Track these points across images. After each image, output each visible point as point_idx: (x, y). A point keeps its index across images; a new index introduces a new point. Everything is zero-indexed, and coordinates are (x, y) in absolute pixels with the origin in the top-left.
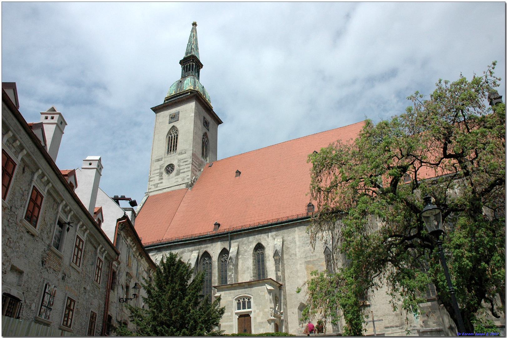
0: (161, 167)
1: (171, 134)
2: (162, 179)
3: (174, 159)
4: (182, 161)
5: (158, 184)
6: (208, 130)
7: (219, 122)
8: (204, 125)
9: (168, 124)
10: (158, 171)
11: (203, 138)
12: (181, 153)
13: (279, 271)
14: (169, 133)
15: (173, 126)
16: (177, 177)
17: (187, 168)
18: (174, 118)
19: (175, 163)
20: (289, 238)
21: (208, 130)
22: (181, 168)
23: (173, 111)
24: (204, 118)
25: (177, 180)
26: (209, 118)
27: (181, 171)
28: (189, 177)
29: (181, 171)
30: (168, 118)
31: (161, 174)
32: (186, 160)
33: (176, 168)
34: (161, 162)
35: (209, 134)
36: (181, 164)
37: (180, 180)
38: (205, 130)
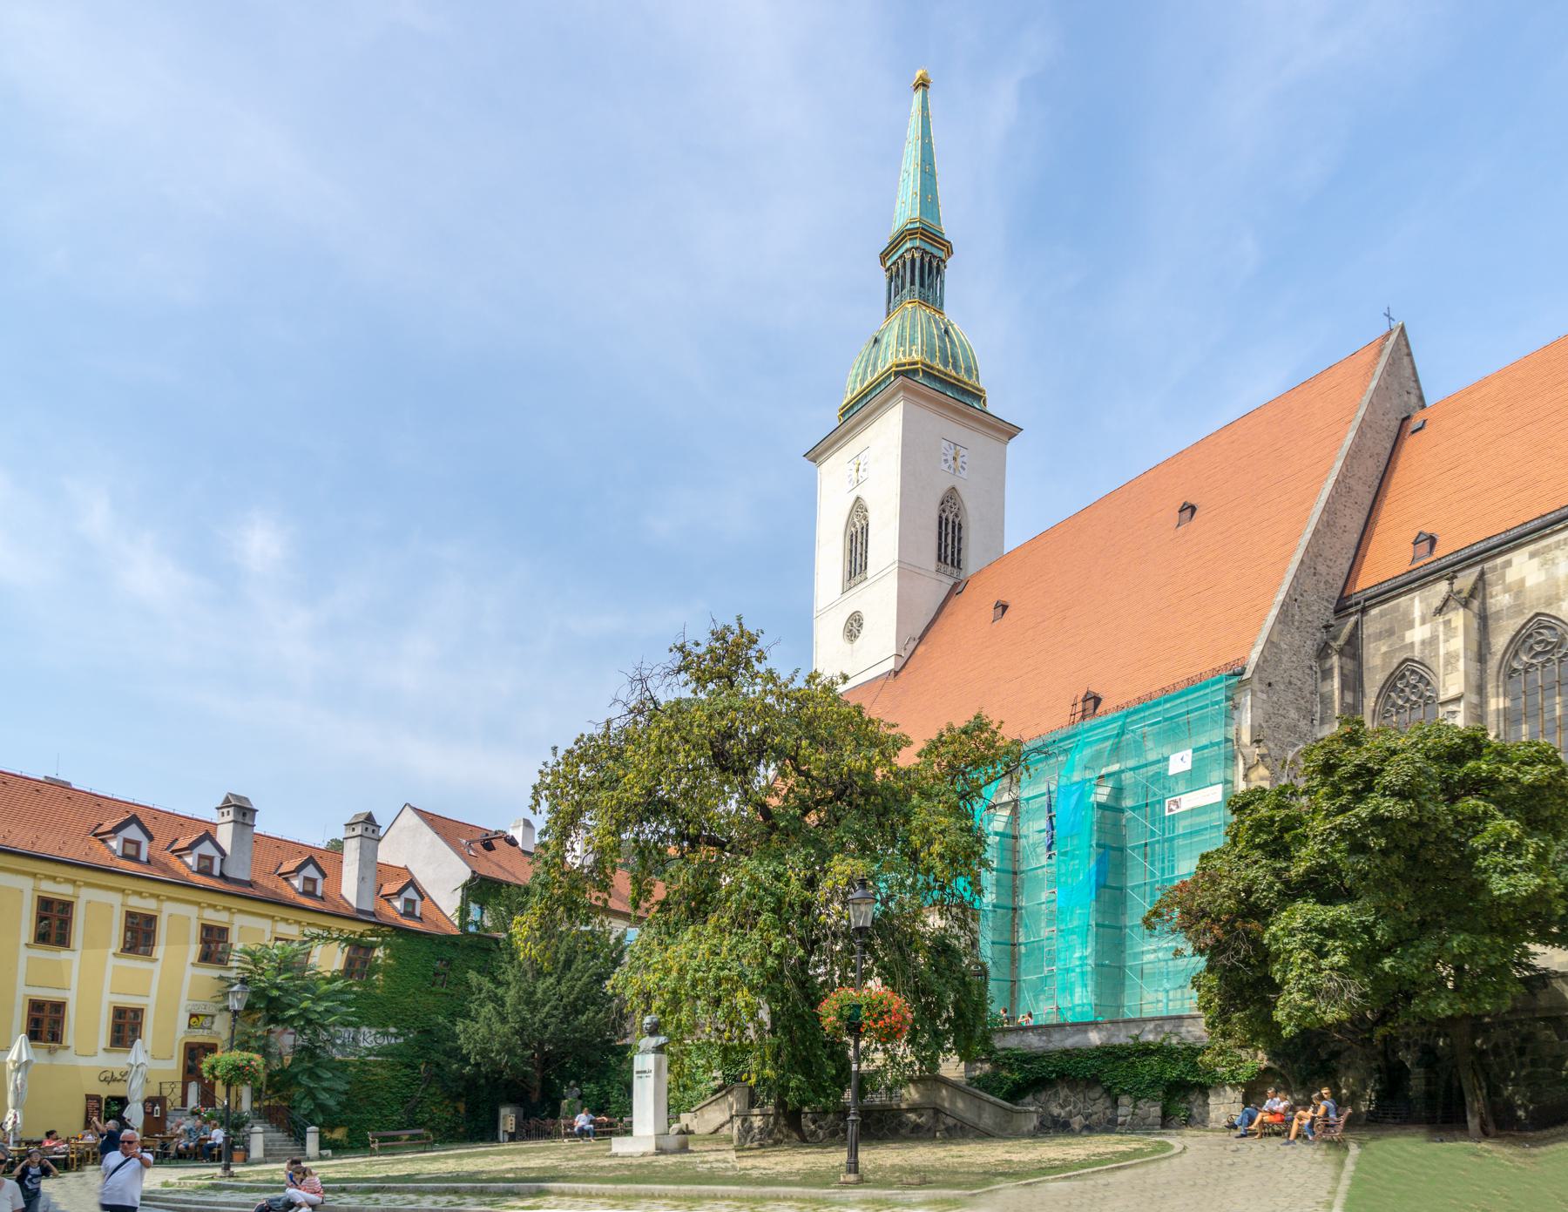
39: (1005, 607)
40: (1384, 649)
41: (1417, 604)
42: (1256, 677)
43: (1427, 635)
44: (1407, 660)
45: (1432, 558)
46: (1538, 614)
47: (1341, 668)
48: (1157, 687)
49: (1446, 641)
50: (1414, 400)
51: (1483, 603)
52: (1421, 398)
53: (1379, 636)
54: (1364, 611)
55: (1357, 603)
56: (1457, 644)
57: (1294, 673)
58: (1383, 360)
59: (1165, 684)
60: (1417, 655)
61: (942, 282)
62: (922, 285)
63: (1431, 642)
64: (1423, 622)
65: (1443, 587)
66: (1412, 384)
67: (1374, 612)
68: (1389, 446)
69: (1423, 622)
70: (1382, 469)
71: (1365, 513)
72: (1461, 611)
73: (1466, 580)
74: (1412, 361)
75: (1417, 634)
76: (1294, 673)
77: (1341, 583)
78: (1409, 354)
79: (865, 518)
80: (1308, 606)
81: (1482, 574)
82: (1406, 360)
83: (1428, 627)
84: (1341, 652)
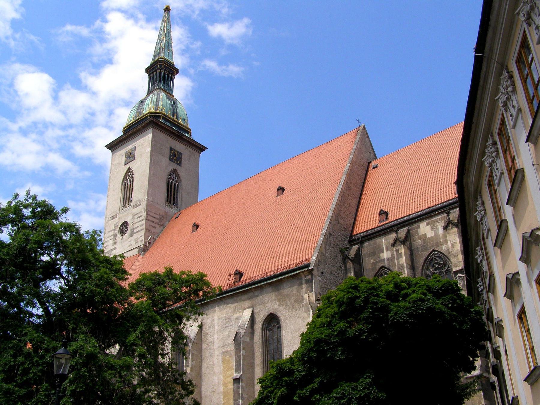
0: (115, 226)
1: (127, 180)
2: (116, 243)
3: (127, 215)
4: (136, 216)
5: (112, 250)
6: (180, 165)
7: (201, 149)
8: (171, 160)
9: (123, 166)
10: (112, 233)
11: (170, 178)
12: (136, 206)
13: (188, 366)
14: (125, 179)
15: (129, 169)
16: (131, 238)
17: (140, 226)
18: (130, 156)
19: (129, 220)
20: (208, 321)
21: (180, 165)
22: (136, 226)
23: (128, 147)
24: (171, 149)
25: (130, 244)
26: (179, 147)
27: (135, 231)
28: (143, 238)
29: (135, 231)
30: (124, 158)
31: (115, 235)
32: (139, 215)
33: (130, 226)
34: (116, 220)
35: (181, 171)
36: (136, 221)
37: (133, 243)
38: (172, 166)
39: (197, 226)
40: (372, 261)
41: (385, 241)
42: (315, 269)
43: (390, 256)
44: (382, 267)
45: (388, 222)
46: (434, 251)
47: (354, 268)
48: (269, 270)
49: (398, 259)
50: (373, 156)
51: (411, 243)
52: (375, 155)
53: (369, 255)
54: (362, 243)
55: (358, 239)
56: (403, 260)
57: (333, 269)
58: (358, 137)
59: (273, 269)
60: (386, 264)
61: (173, 83)
62: (164, 83)
63: (391, 260)
64: (387, 250)
65: (393, 235)
66: (371, 149)
67: (366, 244)
68: (364, 172)
69: (387, 250)
70: (362, 182)
71: (358, 199)
72: (402, 246)
73: (402, 232)
74: (369, 140)
75: (386, 255)
76: (333, 269)
77: (350, 229)
78: (368, 137)
79: (132, 177)
80: (337, 238)
81: (409, 231)
82: (367, 139)
83: (389, 252)
84: (353, 260)
